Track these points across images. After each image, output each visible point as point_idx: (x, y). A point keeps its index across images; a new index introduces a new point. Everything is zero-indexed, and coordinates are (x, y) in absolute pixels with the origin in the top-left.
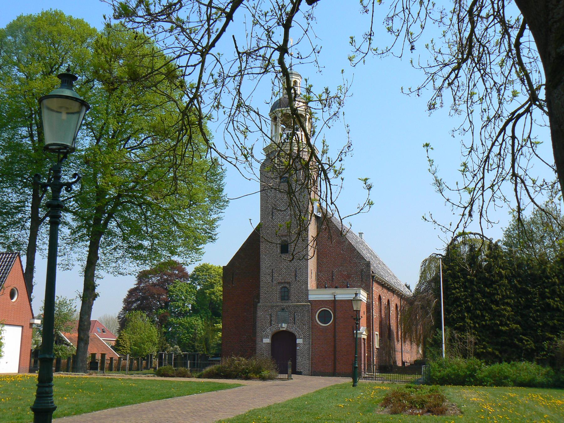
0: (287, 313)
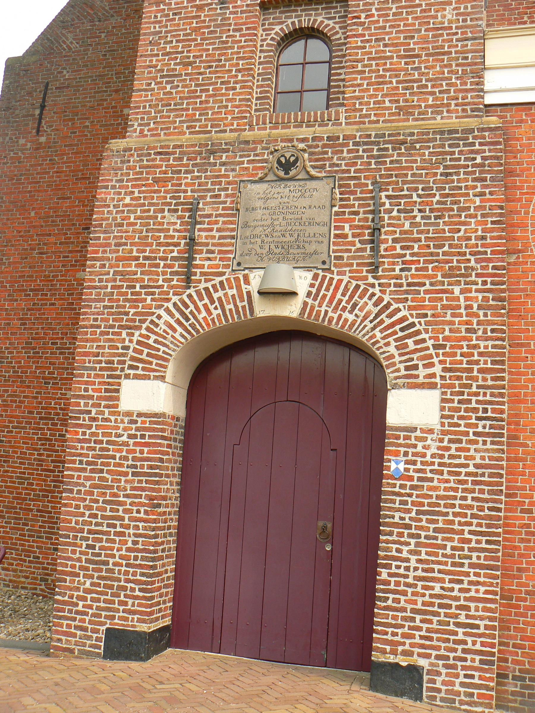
0: (321, 191)
